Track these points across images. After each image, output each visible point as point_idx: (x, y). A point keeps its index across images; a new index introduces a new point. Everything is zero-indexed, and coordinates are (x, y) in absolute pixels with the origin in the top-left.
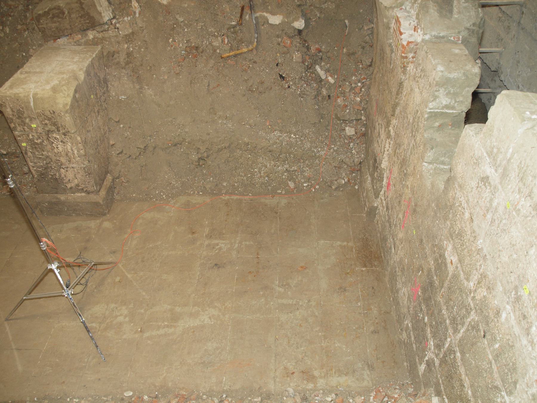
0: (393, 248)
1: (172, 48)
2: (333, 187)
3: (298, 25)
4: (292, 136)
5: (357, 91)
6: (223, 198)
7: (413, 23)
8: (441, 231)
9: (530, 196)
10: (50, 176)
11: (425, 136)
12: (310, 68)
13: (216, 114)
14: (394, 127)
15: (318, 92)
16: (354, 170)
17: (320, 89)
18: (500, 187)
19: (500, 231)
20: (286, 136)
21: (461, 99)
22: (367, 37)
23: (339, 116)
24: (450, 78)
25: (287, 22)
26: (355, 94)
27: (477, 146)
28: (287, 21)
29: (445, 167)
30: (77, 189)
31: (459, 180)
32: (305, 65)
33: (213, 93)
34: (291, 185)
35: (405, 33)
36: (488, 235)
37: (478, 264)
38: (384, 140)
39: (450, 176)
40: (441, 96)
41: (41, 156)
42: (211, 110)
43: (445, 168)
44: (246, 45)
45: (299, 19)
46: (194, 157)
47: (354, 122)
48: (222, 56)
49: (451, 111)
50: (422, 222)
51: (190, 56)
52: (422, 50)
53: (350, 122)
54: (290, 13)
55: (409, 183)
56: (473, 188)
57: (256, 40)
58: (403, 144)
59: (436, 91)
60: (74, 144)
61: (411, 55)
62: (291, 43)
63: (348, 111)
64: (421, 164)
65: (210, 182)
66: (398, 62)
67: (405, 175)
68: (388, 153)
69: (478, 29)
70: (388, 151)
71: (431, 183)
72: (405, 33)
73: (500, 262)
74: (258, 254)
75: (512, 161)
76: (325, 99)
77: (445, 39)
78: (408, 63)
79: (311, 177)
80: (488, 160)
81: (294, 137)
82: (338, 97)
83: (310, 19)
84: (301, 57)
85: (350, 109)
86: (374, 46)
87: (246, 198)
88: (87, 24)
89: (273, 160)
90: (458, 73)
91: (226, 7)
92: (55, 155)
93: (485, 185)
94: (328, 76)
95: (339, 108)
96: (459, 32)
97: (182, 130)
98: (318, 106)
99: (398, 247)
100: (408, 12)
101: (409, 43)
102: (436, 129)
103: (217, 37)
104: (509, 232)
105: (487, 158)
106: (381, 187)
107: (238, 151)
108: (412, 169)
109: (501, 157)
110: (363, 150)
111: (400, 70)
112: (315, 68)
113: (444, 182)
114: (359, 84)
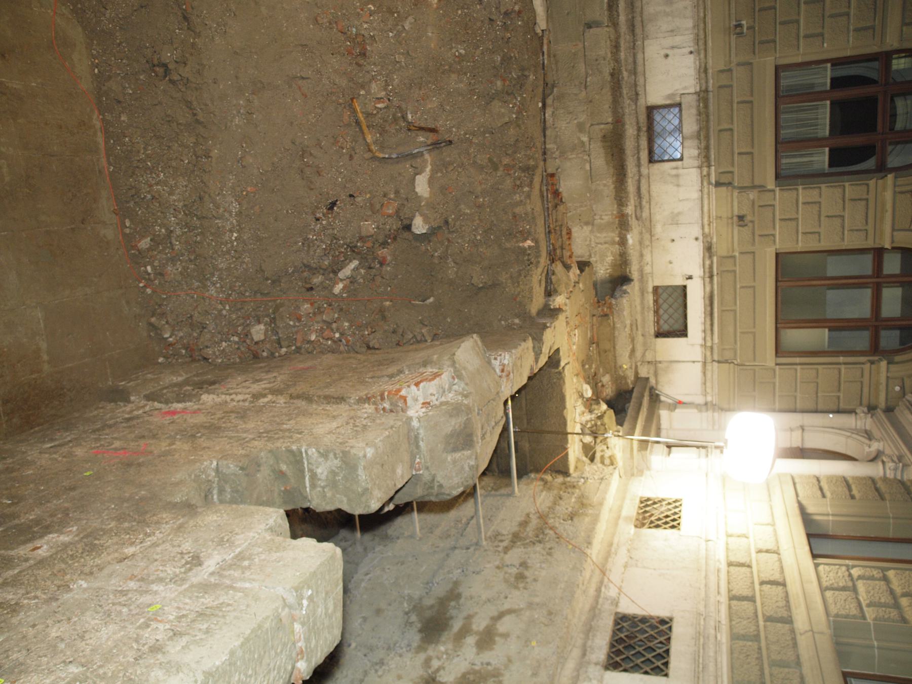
0: (52, 444)
1: (359, 10)
2: (153, 320)
3: (417, 224)
5: (326, 333)
6: (95, 117)
7: (434, 398)
8: (96, 517)
9: (174, 635)
11: (262, 454)
12: (354, 251)
13: (253, 93)
14: (273, 403)
15: (316, 269)
16: (192, 350)
17: (321, 271)
18: (186, 586)
19: (107, 608)
20: (232, 223)
21: (329, 495)
22: (411, 336)
23: (281, 309)
24: (356, 470)
25: (420, 206)
26: (321, 331)
27: (251, 534)
28: (423, 204)
29: (215, 497)
31: (191, 523)
32: (357, 242)
33: (290, 86)
34: (145, 243)
35: (418, 390)
36: (97, 592)
37: (39, 593)
38: (249, 390)
39: (197, 507)
40: (329, 463)
42: (259, 85)
43: (212, 497)
44: (377, 140)
45: (426, 223)
46: (168, 55)
47: (274, 337)
48: (355, 100)
49: (308, 484)
50: (109, 481)
51: (349, 43)
52: (395, 420)
53: (273, 330)
54: (434, 209)
55: (178, 445)
56: (179, 546)
57: (387, 156)
58: (245, 423)
59: (335, 454)
61: (387, 405)
62: (389, 216)
63: (291, 323)
64: (214, 457)
65: (124, 88)
66: (375, 389)
67: (193, 436)
69: (435, 494)
70: (232, 400)
71: (182, 481)
72: (418, 390)
73: (48, 626)
75: (231, 592)
76: (306, 282)
77: (416, 451)
78: (375, 403)
79: (166, 277)
80: (229, 557)
81: (233, 238)
82: (312, 304)
83: (430, 241)
84: (369, 234)
85: (294, 326)
86: (400, 348)
87: (104, 161)
89: (185, 206)
90: (366, 480)
91: (433, 104)
93: (187, 563)
94: (345, 282)
95: (295, 308)
96: (427, 468)
97: (216, 31)
98: (293, 272)
99: (55, 453)
100: (450, 390)
101: (404, 399)
102: (276, 468)
103: (385, 89)
104: (106, 623)
105: (232, 555)
106: (167, 402)
107: (193, 139)
108: (205, 445)
109: (237, 574)
110: (229, 359)
111: (363, 394)
112: (354, 259)
113: (187, 500)
114: (337, 335)
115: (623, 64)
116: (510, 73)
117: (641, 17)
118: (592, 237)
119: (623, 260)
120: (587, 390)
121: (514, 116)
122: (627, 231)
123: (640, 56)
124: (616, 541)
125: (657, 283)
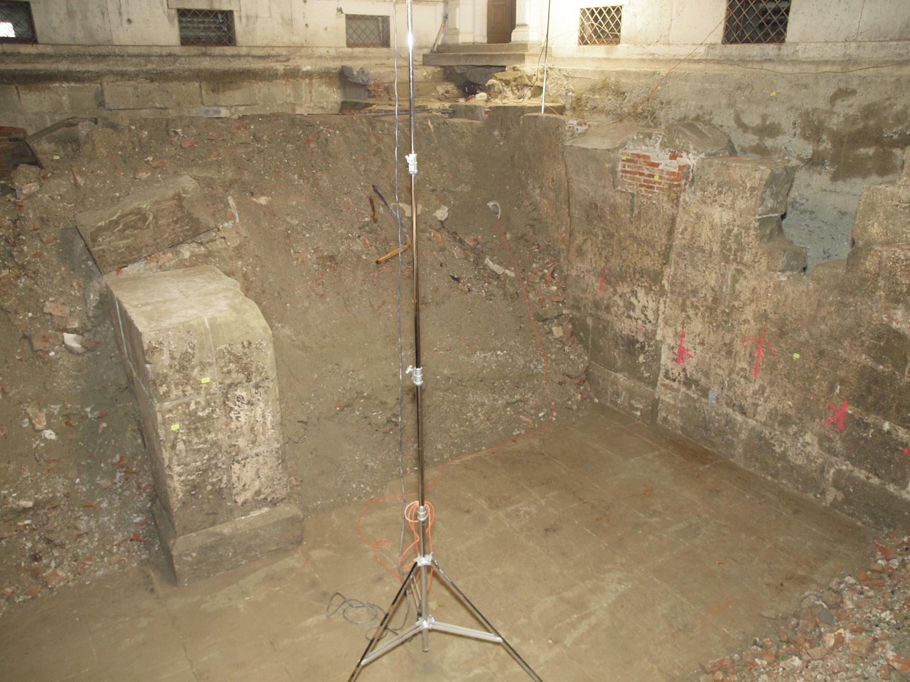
4: (499, 353)
10: (209, 488)
25: (429, 212)
30: (258, 501)
41: (201, 446)
60: (270, 403)
68: (663, 316)
74: (581, 499)
82: (529, 292)
88: (186, 233)
92: (229, 437)
97: (354, 379)
115: (141, 68)
116: (299, 136)
117: (89, 46)
118: (306, 105)
119: (325, 75)
120: (481, 97)
121: (338, 132)
122: (299, 70)
123: (131, 50)
124: (639, 57)
125: (345, 45)
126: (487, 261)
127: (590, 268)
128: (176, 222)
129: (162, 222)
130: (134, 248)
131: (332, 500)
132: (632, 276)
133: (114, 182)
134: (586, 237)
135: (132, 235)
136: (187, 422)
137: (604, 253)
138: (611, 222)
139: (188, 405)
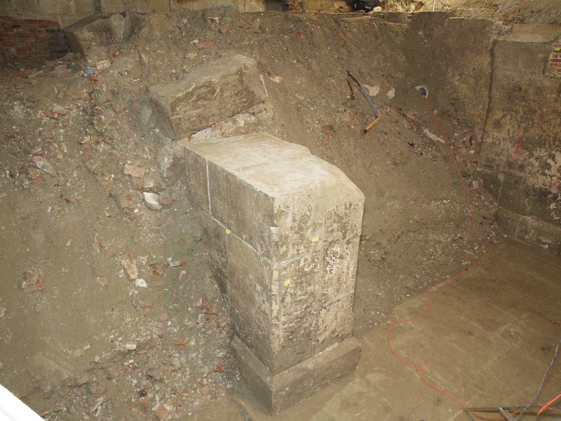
4: (445, 201)
41: (302, 297)
82: (455, 155)
88: (243, 104)
116: (291, 29)
120: (377, 9)
126: (426, 131)
127: (507, 136)
128: (237, 95)
129: (226, 94)
130: (203, 117)
131: (361, 327)
132: (552, 143)
133: (170, 61)
134: (505, 113)
135: (203, 106)
136: (295, 278)
137: (524, 125)
138: (534, 101)
139: (299, 262)
